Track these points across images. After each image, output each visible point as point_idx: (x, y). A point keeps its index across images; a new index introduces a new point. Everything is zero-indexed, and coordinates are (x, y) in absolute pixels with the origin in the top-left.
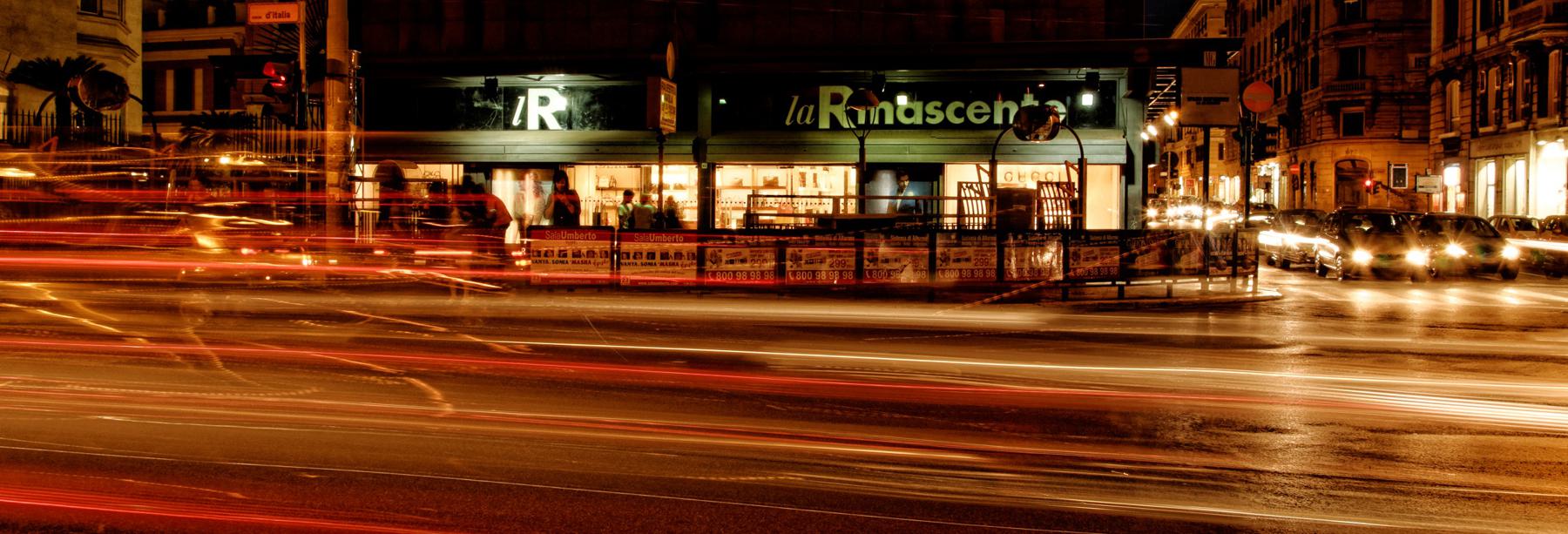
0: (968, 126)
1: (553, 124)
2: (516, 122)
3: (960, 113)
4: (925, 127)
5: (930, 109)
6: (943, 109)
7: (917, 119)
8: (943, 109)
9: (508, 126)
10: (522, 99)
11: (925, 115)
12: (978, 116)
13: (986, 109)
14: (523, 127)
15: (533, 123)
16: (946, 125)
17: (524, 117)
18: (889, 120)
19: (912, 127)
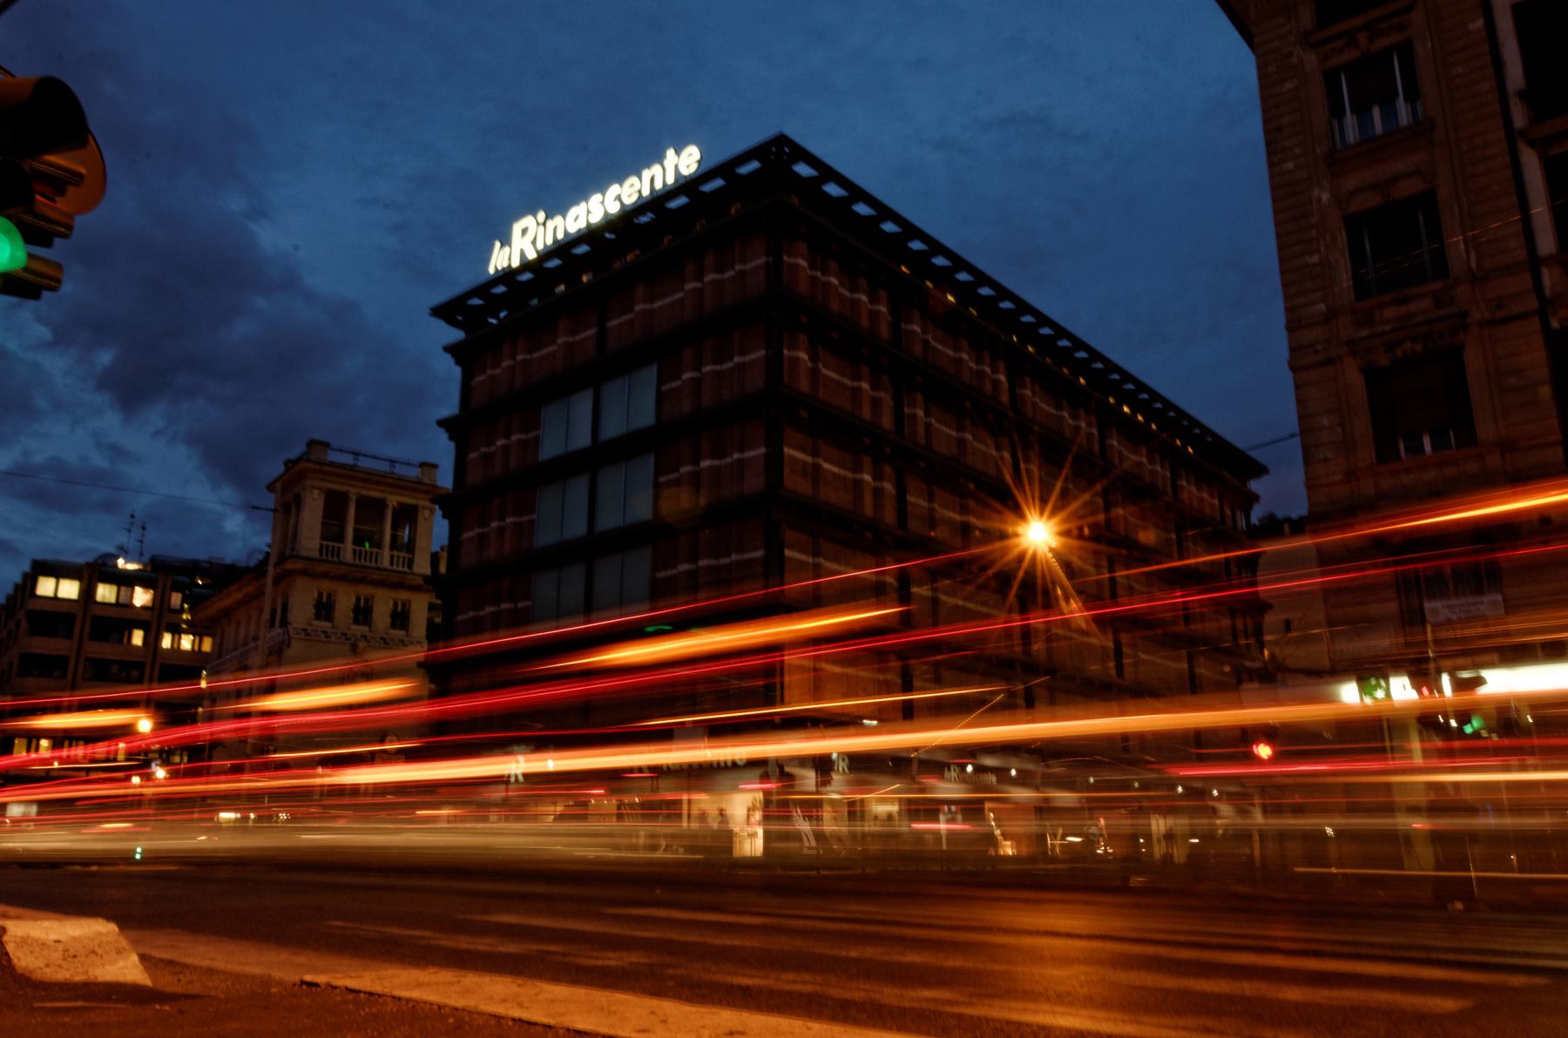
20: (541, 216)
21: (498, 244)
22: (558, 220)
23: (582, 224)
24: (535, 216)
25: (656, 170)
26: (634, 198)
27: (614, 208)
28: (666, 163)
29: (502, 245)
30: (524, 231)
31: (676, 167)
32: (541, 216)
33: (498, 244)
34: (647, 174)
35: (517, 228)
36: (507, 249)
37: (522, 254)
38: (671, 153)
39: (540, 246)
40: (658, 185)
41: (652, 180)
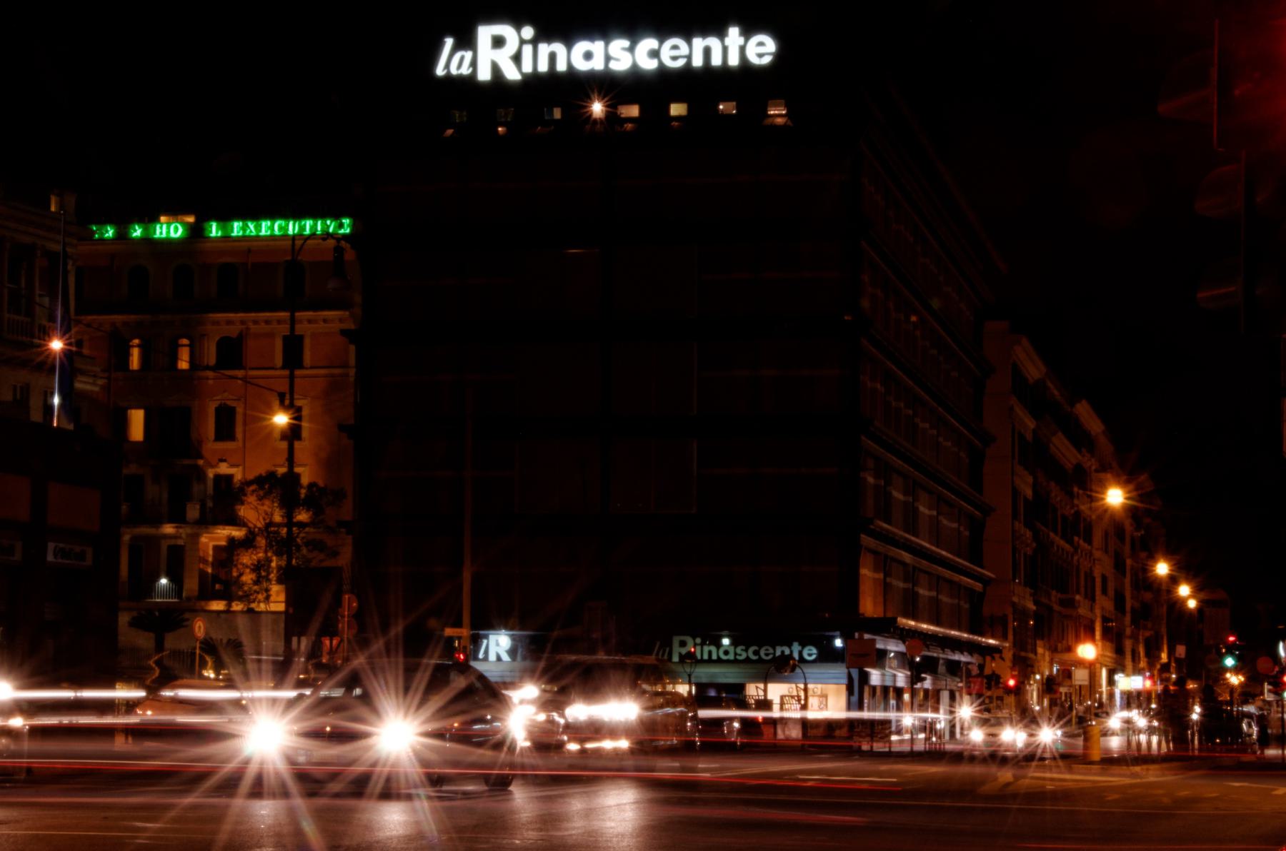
0: (760, 661)
1: (506, 658)
2: (481, 655)
3: (756, 653)
4: (735, 662)
5: (739, 650)
6: (746, 650)
7: (731, 657)
8: (746, 650)
9: (476, 658)
10: (485, 642)
11: (736, 654)
12: (767, 655)
13: (771, 651)
14: (486, 658)
15: (492, 657)
16: (748, 660)
17: (486, 652)
18: (714, 657)
19: (728, 661)
20: (528, 32)
21: (449, 42)
22: (559, 48)
23: (597, 64)
24: (518, 27)
25: (713, 42)
26: (680, 63)
27: (649, 65)
28: (728, 41)
29: (455, 49)
30: (498, 42)
31: (742, 49)
32: (528, 32)
33: (449, 42)
34: (699, 43)
35: (485, 33)
36: (468, 55)
37: (496, 69)
38: (734, 33)
39: (527, 67)
40: (716, 61)
41: (707, 52)
